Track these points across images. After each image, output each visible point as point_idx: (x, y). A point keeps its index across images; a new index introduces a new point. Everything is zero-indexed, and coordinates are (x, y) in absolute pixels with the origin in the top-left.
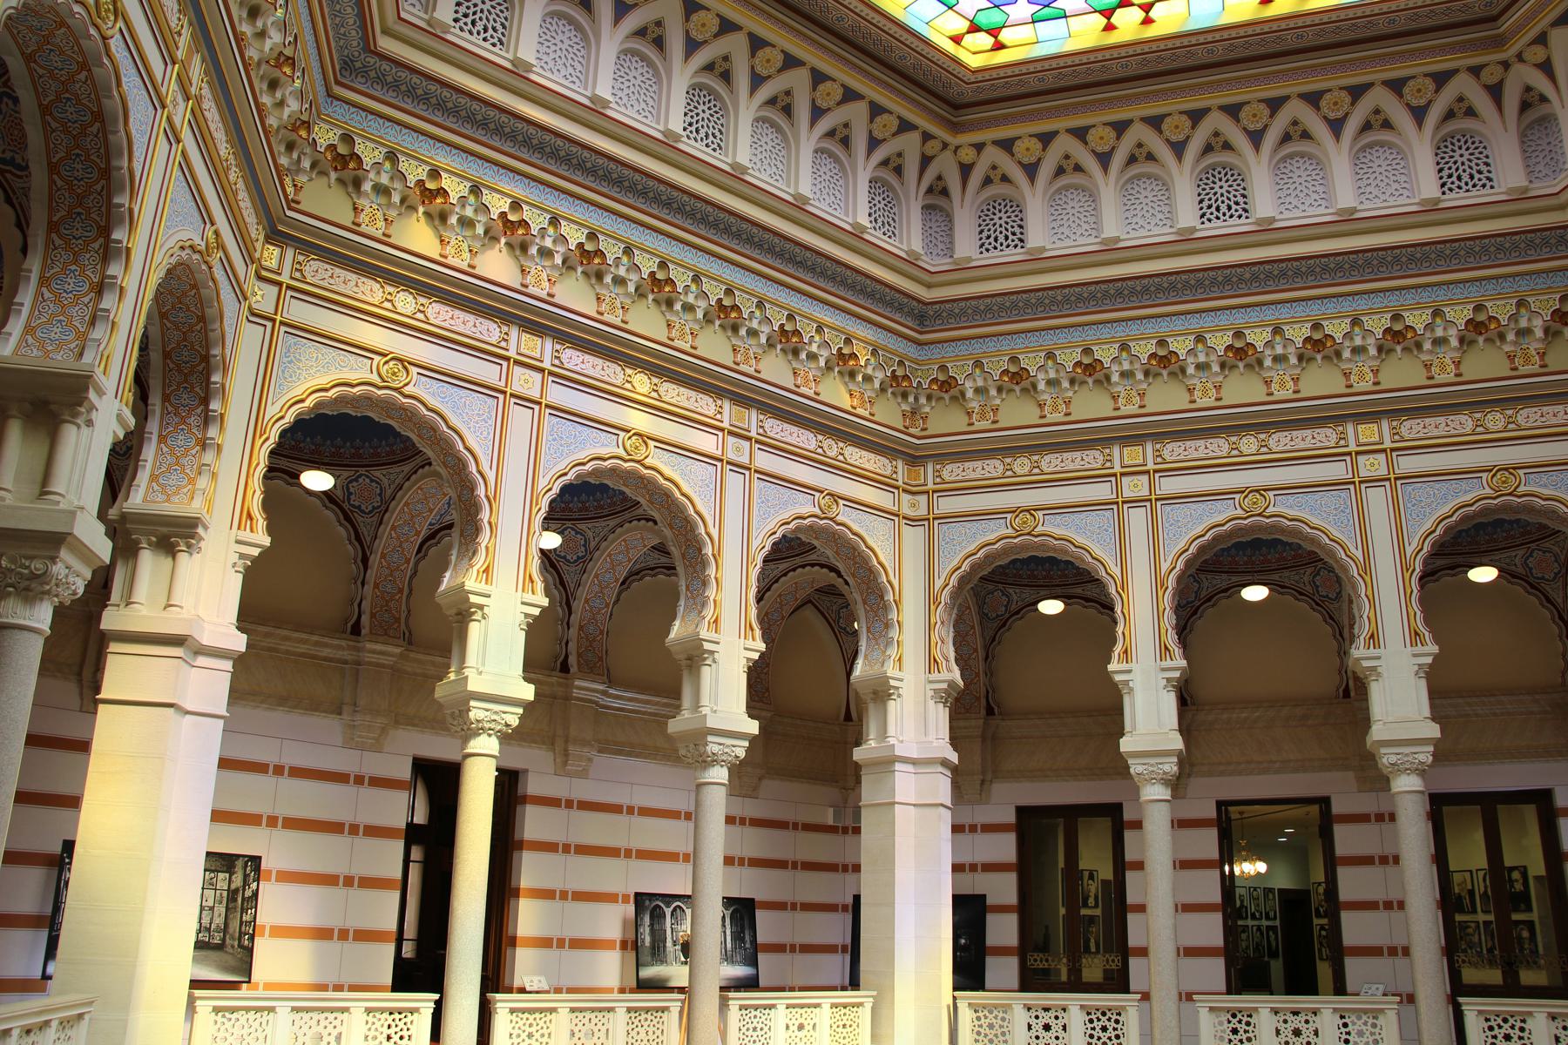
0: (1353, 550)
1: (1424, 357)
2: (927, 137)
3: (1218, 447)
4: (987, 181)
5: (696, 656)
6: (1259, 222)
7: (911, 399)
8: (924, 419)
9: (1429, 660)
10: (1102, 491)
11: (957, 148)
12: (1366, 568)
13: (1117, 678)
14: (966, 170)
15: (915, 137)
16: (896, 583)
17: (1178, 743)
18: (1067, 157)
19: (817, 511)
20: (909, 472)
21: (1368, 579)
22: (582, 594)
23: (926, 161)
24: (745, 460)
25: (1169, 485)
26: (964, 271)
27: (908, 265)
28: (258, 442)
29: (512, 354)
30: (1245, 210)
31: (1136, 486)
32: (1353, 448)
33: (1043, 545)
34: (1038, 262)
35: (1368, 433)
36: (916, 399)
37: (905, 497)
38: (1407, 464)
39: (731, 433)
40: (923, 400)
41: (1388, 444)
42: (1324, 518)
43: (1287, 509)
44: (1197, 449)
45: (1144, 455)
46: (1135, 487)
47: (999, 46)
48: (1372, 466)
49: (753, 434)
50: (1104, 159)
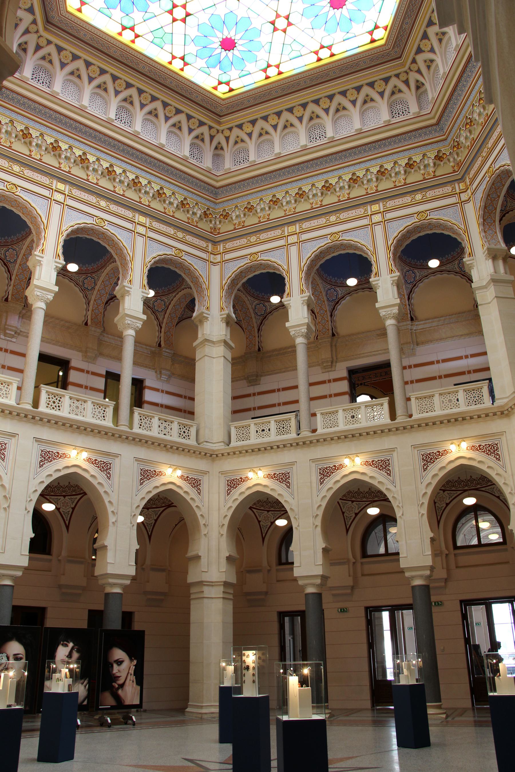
7: (213, 222)
10: (282, 242)
20: (214, 248)
35: (375, 208)
37: (212, 256)
44: (314, 223)
45: (296, 228)
46: (293, 239)
49: (147, 225)
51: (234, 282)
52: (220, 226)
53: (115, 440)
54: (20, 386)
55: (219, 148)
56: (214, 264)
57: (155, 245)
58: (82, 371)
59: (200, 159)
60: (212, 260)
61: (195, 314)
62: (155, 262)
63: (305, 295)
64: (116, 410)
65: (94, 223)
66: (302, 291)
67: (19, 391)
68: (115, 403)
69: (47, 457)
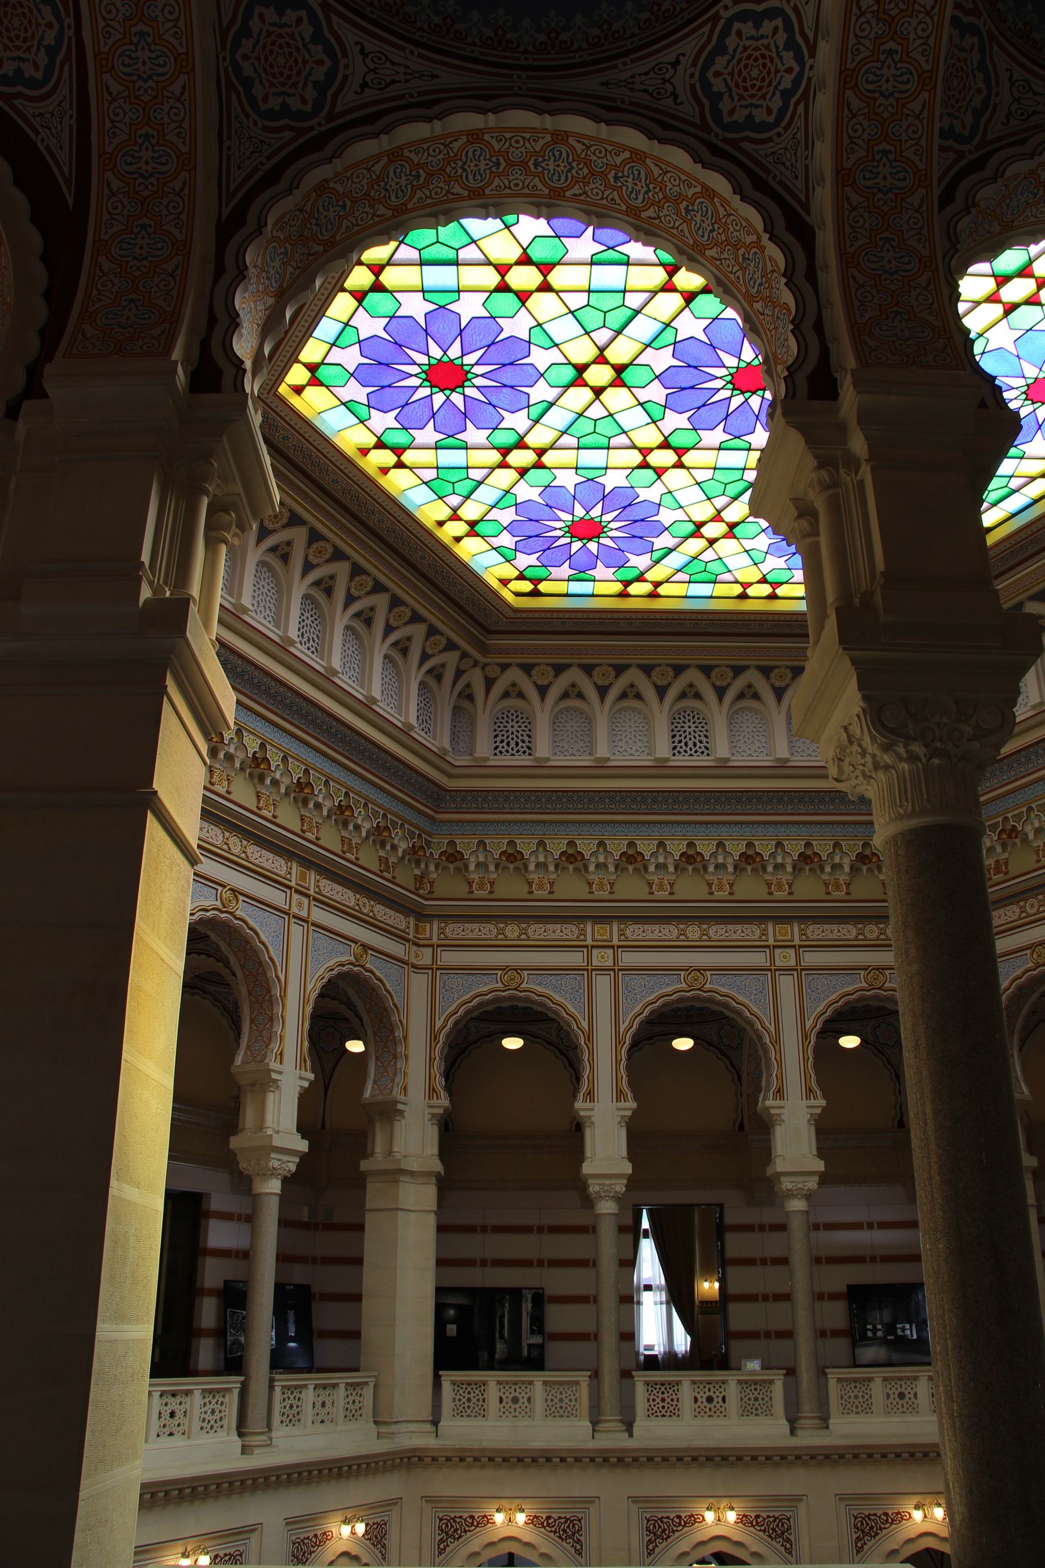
0: (767, 1023)
1: (824, 877)
2: (465, 655)
3: (669, 932)
4: (506, 695)
6: (718, 760)
7: (423, 866)
8: (432, 883)
9: (818, 1111)
10: (575, 959)
11: (485, 665)
12: (777, 1041)
13: (582, 1113)
14: (490, 683)
15: (456, 654)
16: (405, 1022)
17: (628, 1168)
19: (352, 958)
21: (777, 1048)
23: (459, 673)
24: (304, 914)
25: (629, 959)
26: (480, 769)
27: (437, 759)
30: (707, 749)
31: (603, 957)
32: (771, 942)
33: (527, 1000)
34: (542, 769)
36: (427, 866)
38: (811, 958)
40: (432, 868)
41: (797, 942)
42: (746, 997)
43: (719, 987)
44: (653, 932)
45: (613, 932)
46: (602, 958)
47: (535, 593)
48: (786, 958)
49: (312, 892)
50: (603, 691)
52: (434, 876)
57: (323, 941)
63: (627, 1105)
66: (620, 1095)
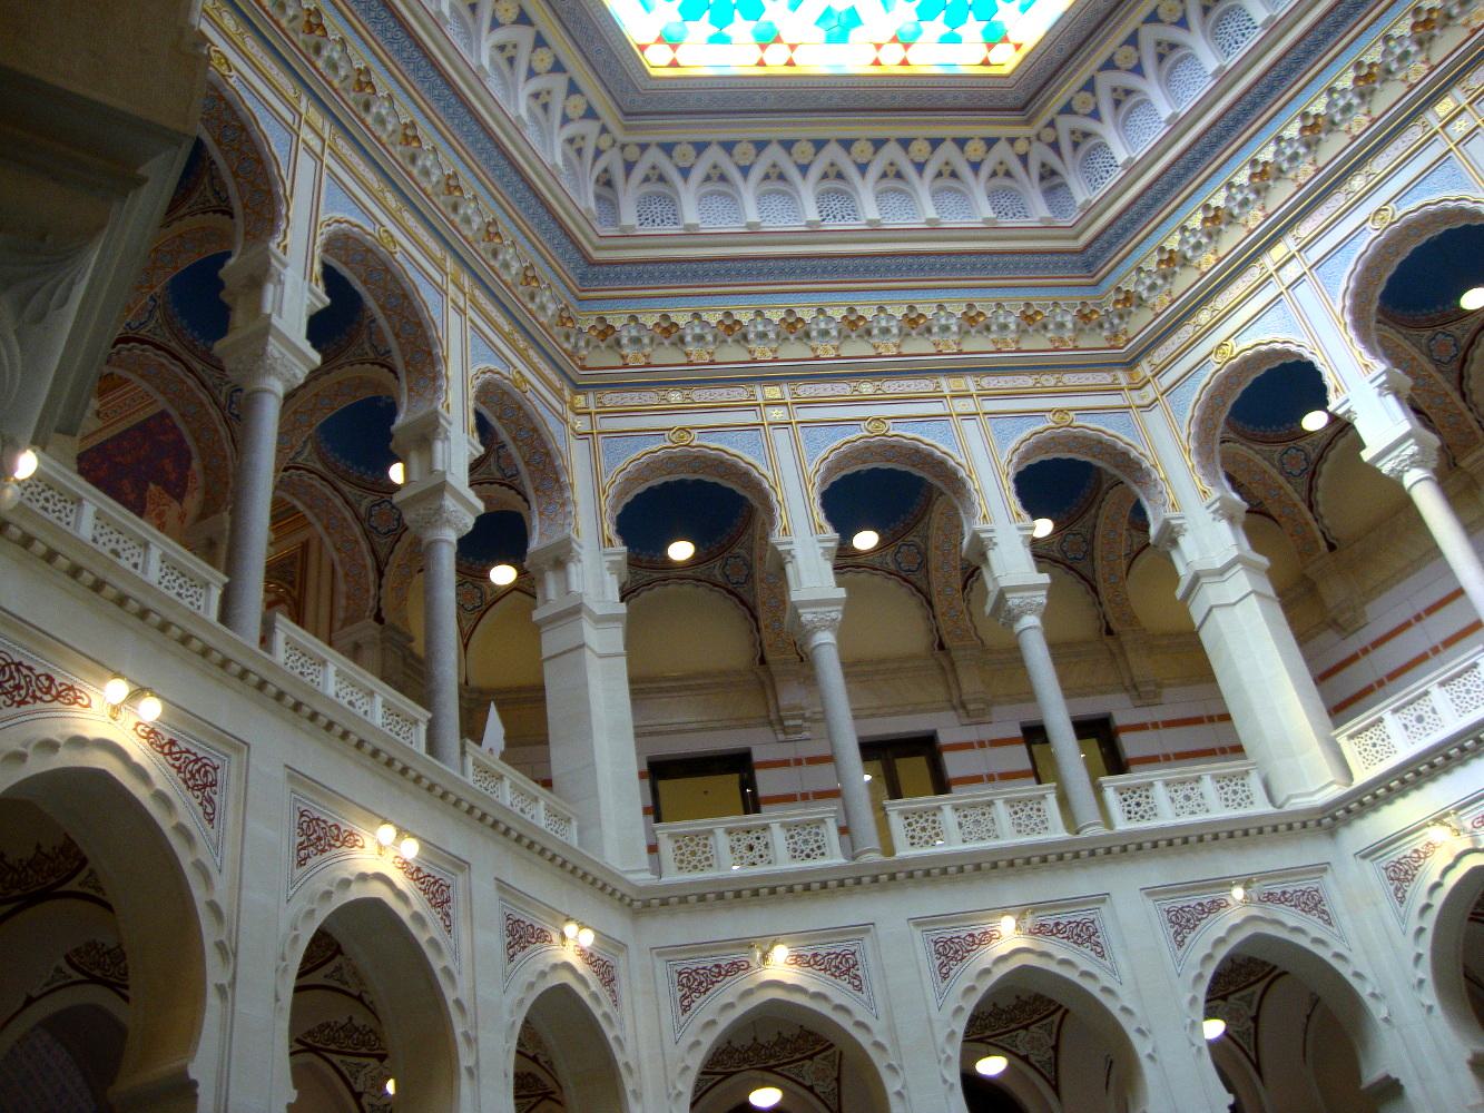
2: (1012, 141)
4: (1076, 145)
5: (981, 549)
7: (1107, 325)
15: (1002, 147)
18: (1115, 90)
22: (934, 592)
23: (1024, 159)
28: (603, 499)
29: (760, 401)
34: (1134, 169)
39: (952, 397)
40: (1116, 321)
51: (1205, 425)
53: (850, 892)
54: (843, 824)
55: (1048, 174)
56: (1149, 407)
58: (968, 746)
59: (1023, 211)
60: (1139, 402)
61: (1153, 531)
62: (1023, 458)
64: (1064, 802)
65: (867, 434)
67: (846, 837)
68: (1054, 784)
69: (694, 984)
